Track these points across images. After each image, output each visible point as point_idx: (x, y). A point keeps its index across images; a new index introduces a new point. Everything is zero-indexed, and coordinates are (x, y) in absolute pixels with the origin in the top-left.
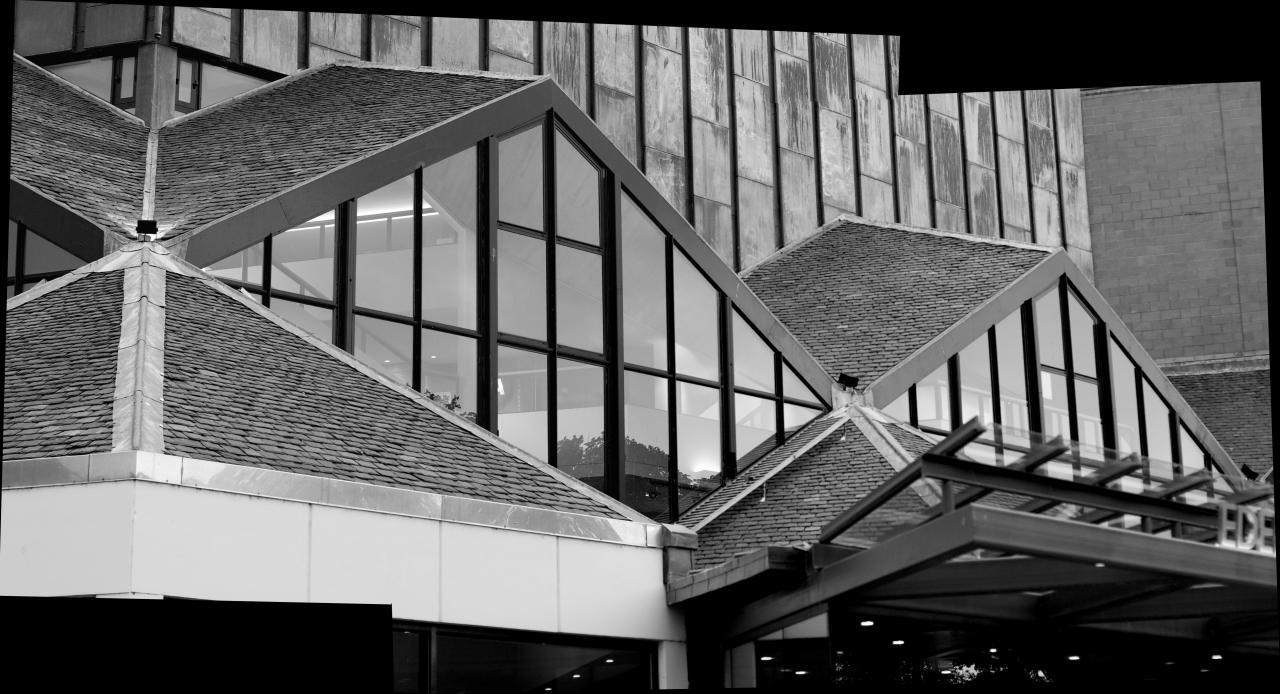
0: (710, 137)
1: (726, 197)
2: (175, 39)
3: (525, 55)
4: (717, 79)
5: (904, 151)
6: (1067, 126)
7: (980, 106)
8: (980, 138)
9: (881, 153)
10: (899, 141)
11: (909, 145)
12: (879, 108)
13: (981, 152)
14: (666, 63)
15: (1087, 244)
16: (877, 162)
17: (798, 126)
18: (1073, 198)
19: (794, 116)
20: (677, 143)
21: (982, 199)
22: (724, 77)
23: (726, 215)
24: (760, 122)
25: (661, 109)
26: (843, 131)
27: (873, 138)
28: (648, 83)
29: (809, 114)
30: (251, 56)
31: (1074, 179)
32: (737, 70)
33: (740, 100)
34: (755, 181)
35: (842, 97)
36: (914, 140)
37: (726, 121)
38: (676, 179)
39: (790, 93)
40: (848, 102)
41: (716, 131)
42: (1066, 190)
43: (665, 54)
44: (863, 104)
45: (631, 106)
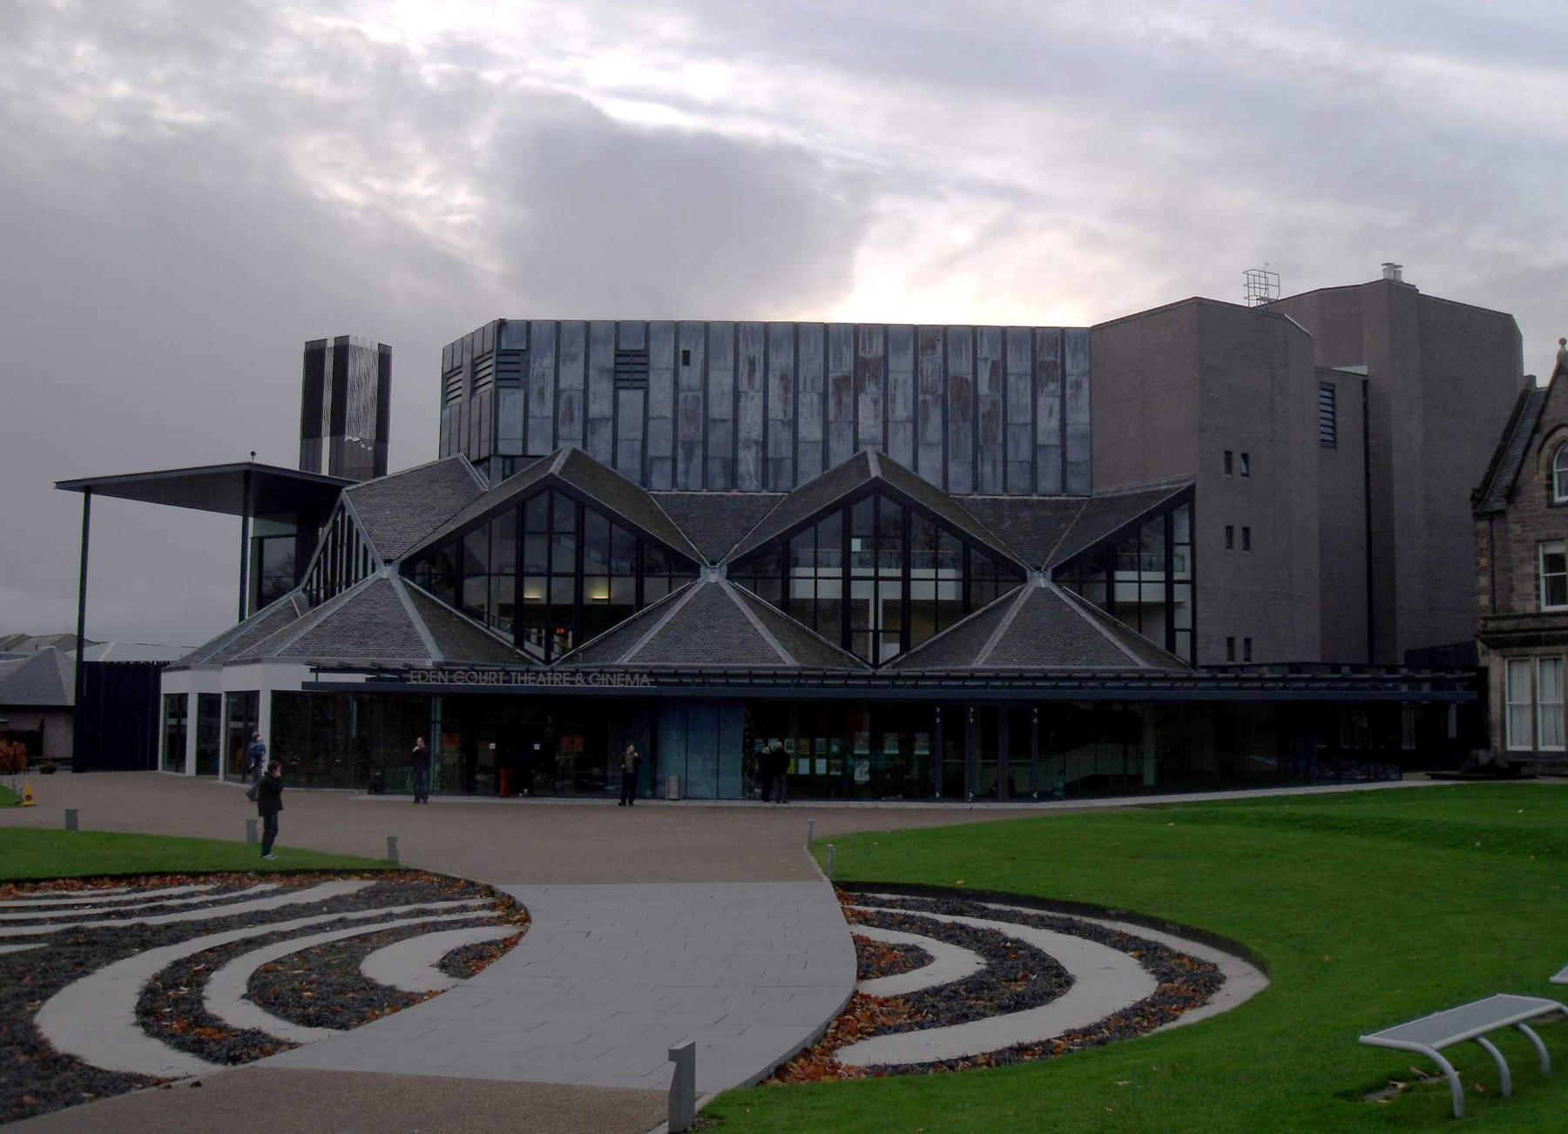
0: (780, 428)
1: (789, 454)
2: (499, 453)
3: (668, 416)
4: (786, 399)
5: (924, 402)
6: (1074, 354)
7: (992, 361)
8: (990, 380)
9: (906, 406)
10: (920, 398)
11: (929, 397)
12: (906, 382)
13: (990, 387)
14: (753, 398)
15: (1087, 420)
16: (901, 410)
17: (843, 407)
18: (1076, 396)
19: (840, 402)
20: (759, 436)
21: (990, 415)
22: (791, 395)
23: (789, 463)
24: (815, 411)
25: (749, 421)
26: (876, 402)
27: (900, 401)
28: (741, 412)
29: (851, 399)
30: (532, 450)
31: (1078, 385)
32: (801, 388)
33: (802, 404)
34: (810, 442)
35: (877, 384)
36: (933, 393)
37: (791, 416)
38: (757, 453)
39: (838, 391)
40: (881, 385)
41: (783, 423)
42: (1069, 392)
43: (751, 394)
44: (893, 383)
45: (730, 425)
